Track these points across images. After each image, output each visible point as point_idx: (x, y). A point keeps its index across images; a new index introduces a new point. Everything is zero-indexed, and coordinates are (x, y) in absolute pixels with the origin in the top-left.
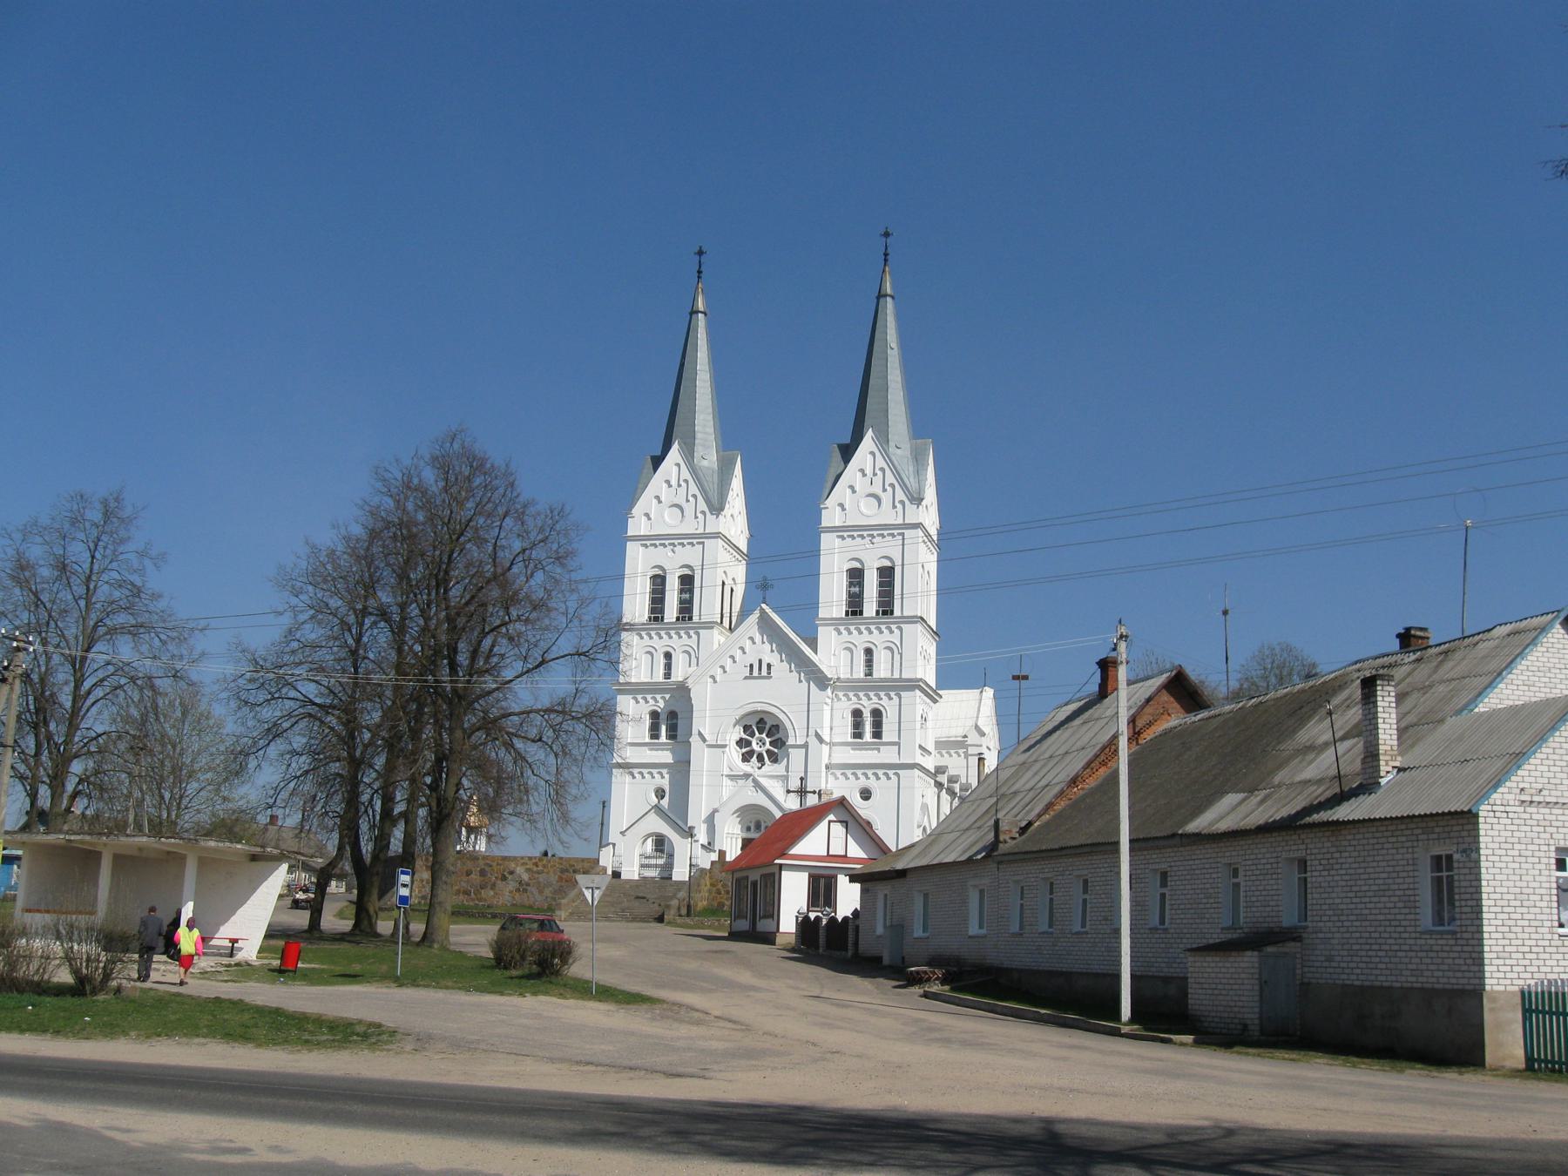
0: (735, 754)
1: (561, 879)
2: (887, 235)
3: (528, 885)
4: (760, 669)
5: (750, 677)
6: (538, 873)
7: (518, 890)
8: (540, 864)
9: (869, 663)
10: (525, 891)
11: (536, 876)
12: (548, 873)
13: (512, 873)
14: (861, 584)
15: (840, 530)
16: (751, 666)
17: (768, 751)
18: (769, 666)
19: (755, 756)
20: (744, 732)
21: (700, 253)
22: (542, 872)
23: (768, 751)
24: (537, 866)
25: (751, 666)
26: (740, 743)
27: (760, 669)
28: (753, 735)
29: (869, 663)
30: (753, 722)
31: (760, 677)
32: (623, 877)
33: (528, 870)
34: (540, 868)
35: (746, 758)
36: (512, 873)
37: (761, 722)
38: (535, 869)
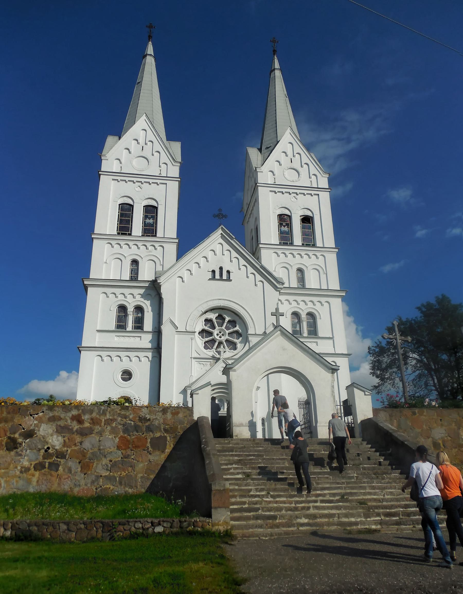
0: (200, 342)
3: (61, 455)
6: (83, 433)
7: (39, 466)
8: (86, 417)
10: (54, 466)
11: (78, 439)
12: (100, 434)
13: (29, 434)
17: (227, 341)
18: (228, 272)
20: (205, 325)
24: (80, 422)
25: (213, 272)
26: (203, 333)
30: (213, 316)
31: (221, 279)
33: (61, 430)
34: (87, 425)
35: (209, 344)
36: (29, 434)
37: (221, 317)
38: (75, 426)
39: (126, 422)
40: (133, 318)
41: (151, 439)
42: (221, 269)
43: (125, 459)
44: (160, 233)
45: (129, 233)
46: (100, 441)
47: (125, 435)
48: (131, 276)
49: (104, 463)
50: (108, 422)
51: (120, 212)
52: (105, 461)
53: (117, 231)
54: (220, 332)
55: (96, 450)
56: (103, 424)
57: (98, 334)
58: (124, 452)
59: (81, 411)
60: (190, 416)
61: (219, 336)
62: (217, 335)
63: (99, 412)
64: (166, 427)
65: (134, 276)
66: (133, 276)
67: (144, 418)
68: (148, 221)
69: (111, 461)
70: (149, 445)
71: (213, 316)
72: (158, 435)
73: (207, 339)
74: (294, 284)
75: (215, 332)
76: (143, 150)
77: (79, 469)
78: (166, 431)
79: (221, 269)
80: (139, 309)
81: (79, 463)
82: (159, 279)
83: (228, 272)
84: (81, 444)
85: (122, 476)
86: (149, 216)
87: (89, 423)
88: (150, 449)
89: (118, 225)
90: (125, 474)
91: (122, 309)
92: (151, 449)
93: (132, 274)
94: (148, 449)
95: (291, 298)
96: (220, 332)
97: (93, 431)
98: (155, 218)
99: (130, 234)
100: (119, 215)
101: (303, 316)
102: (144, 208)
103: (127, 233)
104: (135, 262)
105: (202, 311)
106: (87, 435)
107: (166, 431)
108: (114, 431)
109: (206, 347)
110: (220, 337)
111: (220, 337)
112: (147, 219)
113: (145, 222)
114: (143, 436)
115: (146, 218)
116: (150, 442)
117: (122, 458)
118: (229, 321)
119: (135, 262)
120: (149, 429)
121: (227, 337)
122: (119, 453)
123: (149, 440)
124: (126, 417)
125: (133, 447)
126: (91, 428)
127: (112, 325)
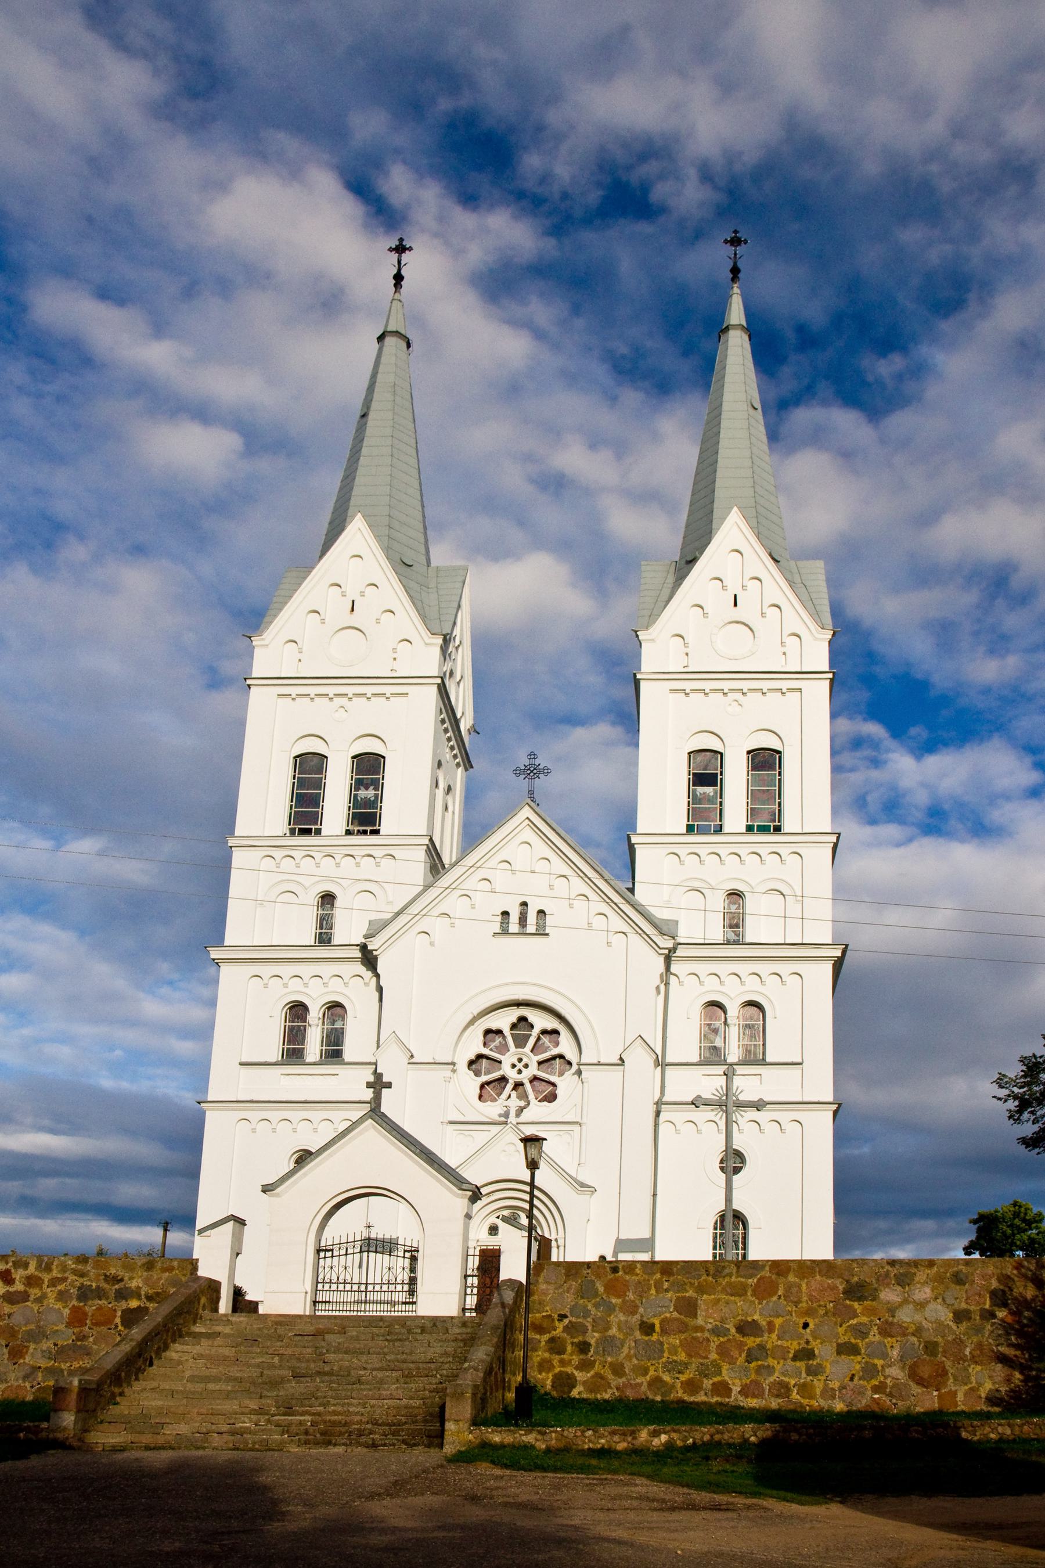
0: (471, 1083)
1: (77, 1318)
4: (523, 920)
5: (505, 932)
12: (39, 1300)
15: (665, 676)
16: (505, 914)
17: (535, 1079)
19: (510, 1086)
22: (24, 1297)
27: (523, 920)
30: (504, 1020)
32: (262, 1310)
34: (19, 1287)
39: (82, 1284)
40: (323, 1032)
41: (123, 1311)
43: (79, 1343)
44: (386, 825)
45: (316, 827)
46: (39, 1313)
47: (81, 1304)
48: (320, 934)
49: (44, 1348)
50: (53, 1283)
51: (297, 776)
52: (47, 1345)
53: (290, 824)
54: (520, 1060)
55: (33, 1327)
56: (45, 1286)
57: (245, 1070)
58: (76, 1330)
59: (10, 1264)
60: (192, 1274)
61: (516, 1069)
62: (514, 1066)
63: (40, 1266)
64: (150, 1291)
66: (325, 933)
67: (113, 1277)
68: (362, 793)
69: (55, 1345)
70: (118, 1320)
71: (504, 1020)
72: (134, 1304)
73: (485, 1078)
75: (507, 1060)
77: (6, 1356)
78: (150, 1298)
80: (335, 1009)
81: (7, 1346)
82: (371, 941)
84: (9, 1318)
85: (72, 1368)
86: (365, 782)
87: (24, 1284)
88: (120, 1328)
89: (291, 809)
90: (78, 1366)
91: (298, 1010)
92: (122, 1329)
93: (321, 928)
94: (116, 1326)
97: (29, 1296)
98: (377, 784)
99: (318, 832)
100: (294, 783)
102: (353, 761)
103: (313, 827)
104: (328, 899)
105: (472, 1013)
106: (18, 1303)
107: (150, 1298)
108: (62, 1296)
110: (520, 1072)
111: (520, 1072)
112: (362, 788)
113: (356, 796)
114: (110, 1306)
115: (359, 785)
116: (122, 1317)
117: (73, 1341)
119: (328, 899)
120: (123, 1295)
121: (533, 1070)
122: (70, 1331)
123: (119, 1313)
124: (82, 1275)
125: (93, 1324)
126: (25, 1291)
127: (274, 1049)
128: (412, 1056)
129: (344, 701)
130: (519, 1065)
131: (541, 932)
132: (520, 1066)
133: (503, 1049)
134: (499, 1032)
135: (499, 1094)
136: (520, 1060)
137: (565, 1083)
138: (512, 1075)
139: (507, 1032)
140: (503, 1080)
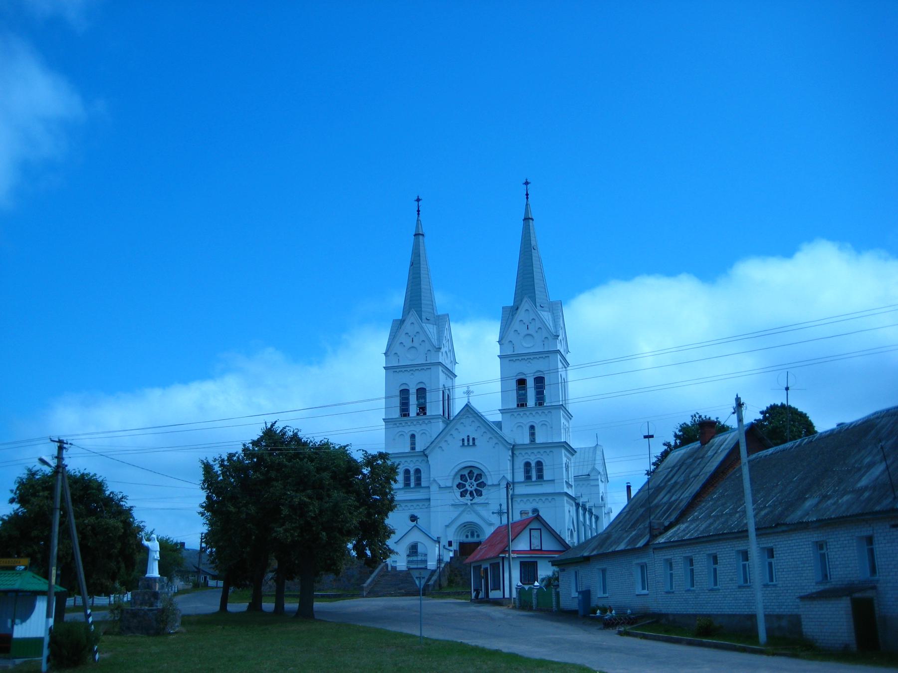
0: (457, 492)
2: (527, 183)
9: (532, 434)
14: (525, 389)
16: (463, 440)
18: (474, 439)
19: (468, 493)
21: (418, 200)
23: (476, 490)
25: (463, 440)
26: (459, 486)
28: (466, 481)
29: (532, 434)
30: (466, 472)
37: (471, 472)
42: (468, 436)
62: (469, 486)
65: (413, 448)
71: (466, 472)
74: (527, 441)
75: (467, 484)
76: (413, 341)
79: (468, 436)
80: (418, 471)
83: (474, 439)
95: (523, 452)
96: (471, 484)
101: (533, 464)
104: (413, 436)
109: (461, 496)
110: (471, 487)
111: (471, 487)
118: (477, 475)
119: (413, 436)
128: (440, 485)
129: (411, 372)
130: (471, 485)
131: (474, 444)
132: (471, 485)
133: (466, 481)
134: (465, 475)
135: (466, 494)
136: (471, 484)
137: (484, 491)
138: (469, 489)
139: (467, 475)
140: (467, 490)
